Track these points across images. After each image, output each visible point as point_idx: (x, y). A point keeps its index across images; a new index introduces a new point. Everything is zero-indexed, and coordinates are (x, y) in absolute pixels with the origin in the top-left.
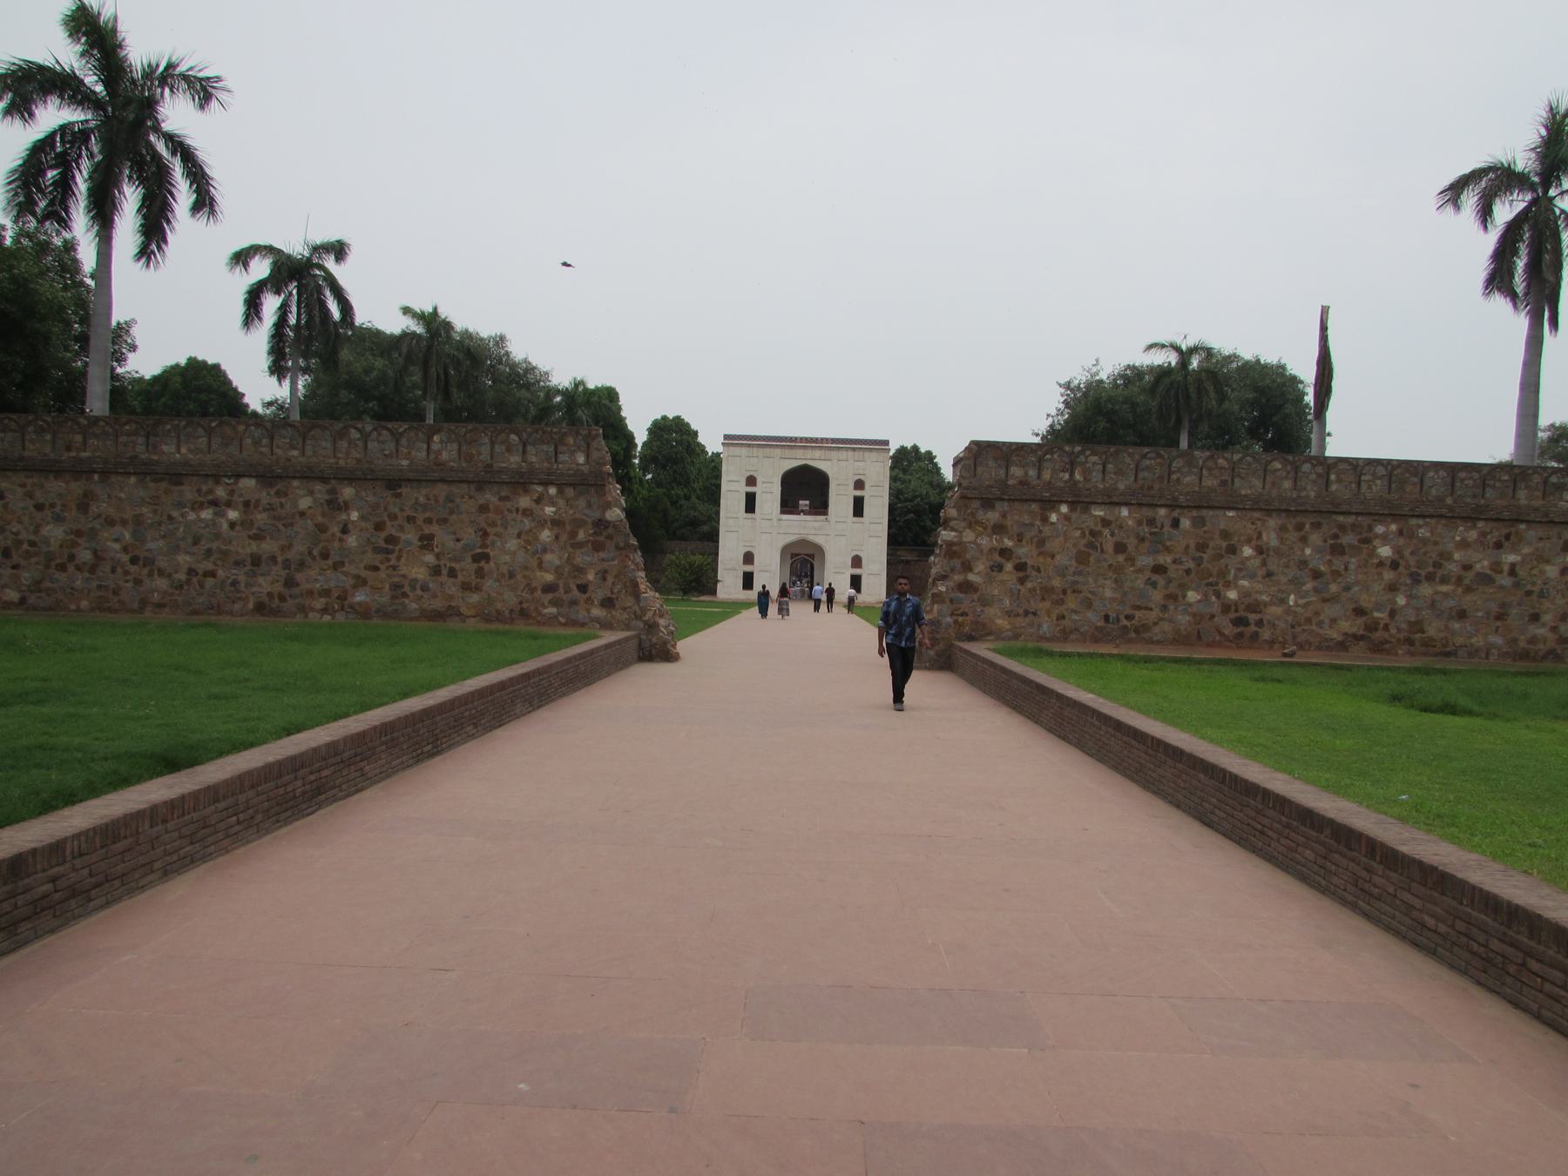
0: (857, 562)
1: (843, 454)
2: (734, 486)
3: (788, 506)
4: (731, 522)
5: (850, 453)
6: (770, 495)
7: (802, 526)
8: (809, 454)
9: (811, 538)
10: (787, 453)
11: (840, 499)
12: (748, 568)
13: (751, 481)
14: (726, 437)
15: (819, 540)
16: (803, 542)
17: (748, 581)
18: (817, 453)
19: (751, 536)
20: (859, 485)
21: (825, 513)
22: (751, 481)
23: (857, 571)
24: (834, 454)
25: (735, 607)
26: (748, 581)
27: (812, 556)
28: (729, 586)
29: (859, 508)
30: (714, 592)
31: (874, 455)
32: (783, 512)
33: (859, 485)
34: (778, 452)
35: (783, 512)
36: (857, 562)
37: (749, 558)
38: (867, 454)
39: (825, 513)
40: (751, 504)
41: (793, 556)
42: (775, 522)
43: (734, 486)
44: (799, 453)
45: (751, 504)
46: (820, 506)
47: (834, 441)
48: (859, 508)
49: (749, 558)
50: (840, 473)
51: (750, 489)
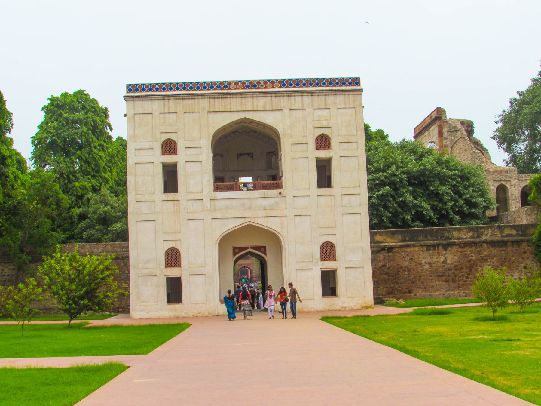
0: (328, 251)
1: (297, 101)
2: (145, 156)
3: (224, 179)
4: (144, 208)
5: (307, 99)
6: (197, 166)
7: (247, 205)
8: (249, 103)
9: (261, 222)
10: (218, 104)
11: (297, 165)
12: (173, 272)
13: (169, 147)
14: (130, 88)
15: (271, 224)
16: (250, 229)
17: (174, 291)
18: (261, 102)
19: (176, 225)
20: (323, 142)
21: (278, 186)
22: (169, 147)
23: (329, 265)
24: (283, 102)
25: (159, 333)
26: (174, 291)
27: (263, 249)
28: (147, 302)
29: (324, 176)
30: (125, 309)
31: (340, 99)
32: (217, 189)
33: (323, 142)
34: (205, 103)
35: (217, 189)
36: (328, 251)
37: (173, 257)
38: (330, 99)
39: (278, 186)
40: (170, 179)
41: (237, 250)
42: (207, 203)
43: (145, 156)
44: (235, 103)
45: (170, 179)
46: (270, 176)
47: (283, 83)
48: (324, 176)
49: (173, 257)
50: (293, 126)
51: (169, 159)
